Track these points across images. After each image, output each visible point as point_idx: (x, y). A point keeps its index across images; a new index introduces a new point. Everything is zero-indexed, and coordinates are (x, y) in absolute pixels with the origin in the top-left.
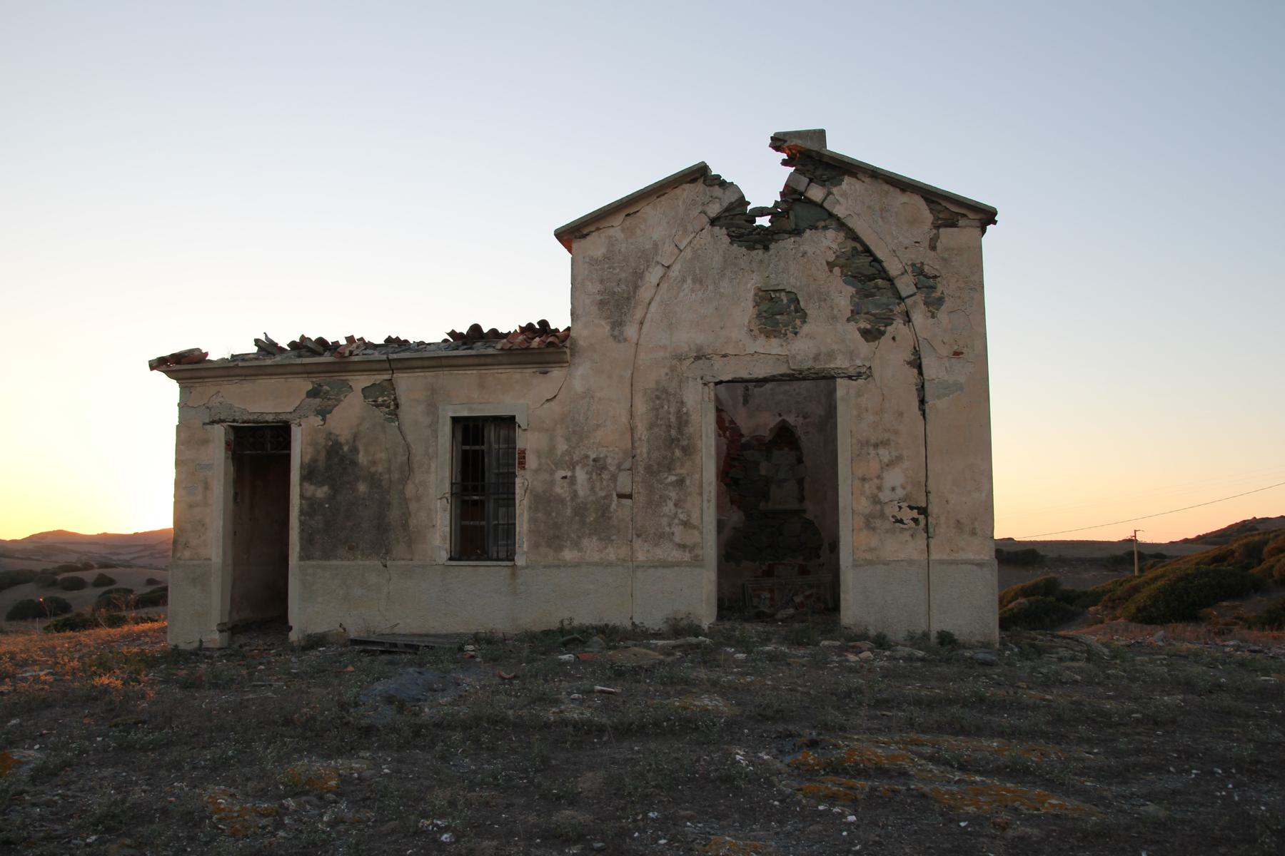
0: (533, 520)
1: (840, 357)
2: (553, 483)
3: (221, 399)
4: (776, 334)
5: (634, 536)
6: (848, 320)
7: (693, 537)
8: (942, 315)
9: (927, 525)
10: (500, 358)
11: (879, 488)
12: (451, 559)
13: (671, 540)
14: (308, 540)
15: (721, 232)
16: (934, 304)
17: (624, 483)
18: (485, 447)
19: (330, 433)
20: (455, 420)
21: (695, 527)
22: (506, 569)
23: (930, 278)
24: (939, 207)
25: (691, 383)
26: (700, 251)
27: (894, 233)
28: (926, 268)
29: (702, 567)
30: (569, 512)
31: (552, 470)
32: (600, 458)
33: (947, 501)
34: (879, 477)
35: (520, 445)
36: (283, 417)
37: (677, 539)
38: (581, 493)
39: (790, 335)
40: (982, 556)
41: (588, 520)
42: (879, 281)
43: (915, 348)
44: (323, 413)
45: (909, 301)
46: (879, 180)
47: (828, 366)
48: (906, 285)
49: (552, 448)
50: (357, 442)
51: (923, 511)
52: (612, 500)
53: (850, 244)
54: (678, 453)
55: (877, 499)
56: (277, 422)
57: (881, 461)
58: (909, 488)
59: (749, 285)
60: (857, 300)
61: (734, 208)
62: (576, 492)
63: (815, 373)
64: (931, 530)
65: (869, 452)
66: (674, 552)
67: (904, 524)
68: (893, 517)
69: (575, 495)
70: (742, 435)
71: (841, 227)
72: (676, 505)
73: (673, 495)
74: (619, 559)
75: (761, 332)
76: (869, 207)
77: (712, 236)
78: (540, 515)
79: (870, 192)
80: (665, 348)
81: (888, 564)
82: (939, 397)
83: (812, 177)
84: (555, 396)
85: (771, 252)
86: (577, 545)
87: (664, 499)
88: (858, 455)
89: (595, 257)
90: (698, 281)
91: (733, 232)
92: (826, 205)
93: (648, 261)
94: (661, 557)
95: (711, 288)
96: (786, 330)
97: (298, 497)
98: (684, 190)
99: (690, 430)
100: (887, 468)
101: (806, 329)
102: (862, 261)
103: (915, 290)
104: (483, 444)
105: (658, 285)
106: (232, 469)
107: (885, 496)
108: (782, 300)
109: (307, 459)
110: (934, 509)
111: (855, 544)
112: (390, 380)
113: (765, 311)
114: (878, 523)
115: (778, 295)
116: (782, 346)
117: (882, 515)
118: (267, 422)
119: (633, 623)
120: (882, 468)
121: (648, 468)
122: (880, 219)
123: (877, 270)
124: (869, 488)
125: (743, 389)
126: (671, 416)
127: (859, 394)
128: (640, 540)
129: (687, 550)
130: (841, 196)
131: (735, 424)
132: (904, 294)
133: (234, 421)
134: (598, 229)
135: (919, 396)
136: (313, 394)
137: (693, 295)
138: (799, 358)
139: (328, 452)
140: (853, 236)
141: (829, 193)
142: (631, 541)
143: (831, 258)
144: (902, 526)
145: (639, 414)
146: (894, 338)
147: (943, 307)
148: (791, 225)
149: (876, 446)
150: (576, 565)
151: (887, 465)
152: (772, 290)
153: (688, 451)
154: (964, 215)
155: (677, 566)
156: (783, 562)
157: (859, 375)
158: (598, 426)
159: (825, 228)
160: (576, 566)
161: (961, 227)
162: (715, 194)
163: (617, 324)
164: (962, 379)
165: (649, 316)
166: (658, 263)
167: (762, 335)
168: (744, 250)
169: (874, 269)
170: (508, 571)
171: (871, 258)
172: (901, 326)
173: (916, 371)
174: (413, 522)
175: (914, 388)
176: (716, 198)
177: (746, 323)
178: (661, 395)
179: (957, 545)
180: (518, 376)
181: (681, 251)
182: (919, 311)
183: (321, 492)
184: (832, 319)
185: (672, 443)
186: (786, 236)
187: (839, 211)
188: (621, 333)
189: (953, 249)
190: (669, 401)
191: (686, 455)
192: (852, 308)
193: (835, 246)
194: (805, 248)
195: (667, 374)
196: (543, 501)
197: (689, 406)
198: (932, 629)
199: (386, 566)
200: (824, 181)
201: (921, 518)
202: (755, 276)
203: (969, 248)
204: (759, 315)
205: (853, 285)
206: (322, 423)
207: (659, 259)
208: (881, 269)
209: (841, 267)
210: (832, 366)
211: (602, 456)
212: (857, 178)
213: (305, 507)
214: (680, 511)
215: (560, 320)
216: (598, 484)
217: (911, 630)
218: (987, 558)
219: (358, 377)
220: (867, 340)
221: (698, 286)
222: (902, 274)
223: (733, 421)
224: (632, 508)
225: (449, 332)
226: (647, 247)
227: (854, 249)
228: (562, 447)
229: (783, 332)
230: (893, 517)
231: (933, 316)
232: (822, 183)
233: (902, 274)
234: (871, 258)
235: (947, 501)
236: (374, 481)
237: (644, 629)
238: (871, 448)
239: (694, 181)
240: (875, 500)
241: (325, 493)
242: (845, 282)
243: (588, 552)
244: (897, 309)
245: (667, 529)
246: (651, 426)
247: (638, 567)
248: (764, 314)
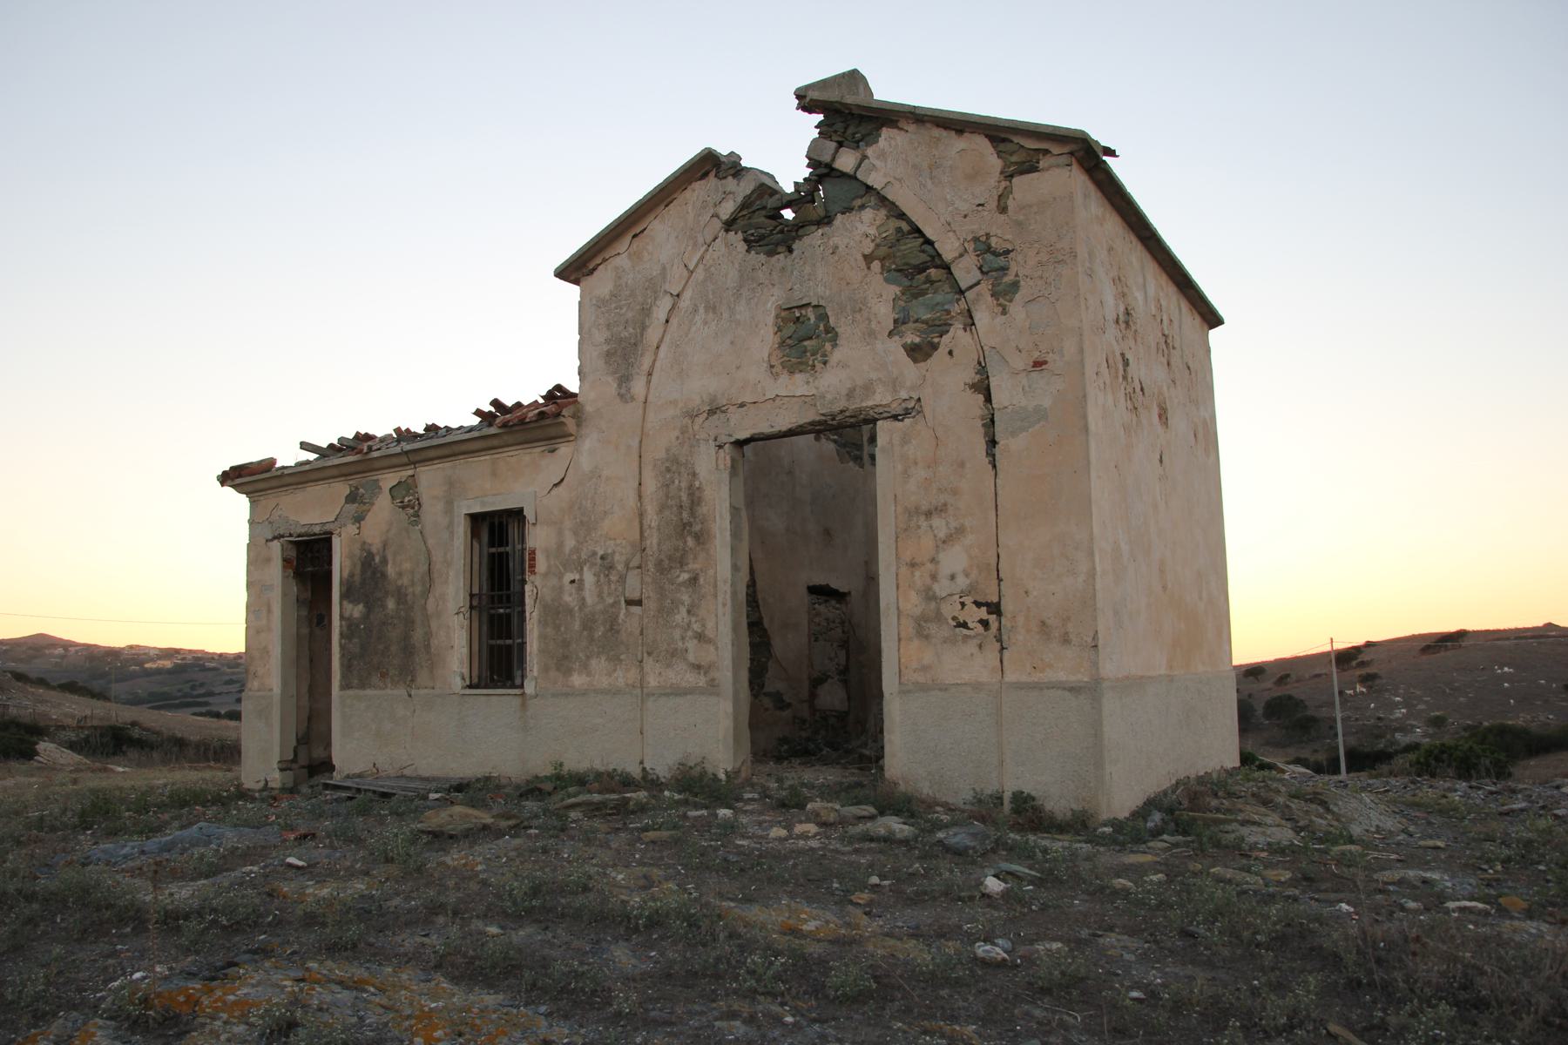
0: (543, 637)
1: (880, 389)
2: (561, 589)
3: (280, 513)
4: (802, 367)
5: (645, 655)
6: (891, 334)
7: (707, 655)
8: (1016, 308)
9: (999, 629)
10: (505, 437)
11: (934, 577)
12: (470, 686)
13: (685, 659)
14: (347, 668)
15: (736, 238)
16: (1004, 293)
17: (633, 587)
18: (508, 549)
19: (364, 543)
20: (476, 519)
21: (710, 641)
23: (1000, 255)
24: (1009, 147)
25: (703, 448)
26: (713, 269)
27: (948, 197)
28: (993, 242)
29: (718, 695)
30: (577, 626)
31: (560, 572)
32: (608, 554)
33: (1026, 592)
34: (933, 560)
37: (691, 657)
38: (589, 601)
39: (819, 366)
40: (1080, 677)
41: (596, 636)
42: (932, 271)
43: (979, 363)
44: (359, 519)
45: (970, 295)
46: (928, 125)
47: (864, 404)
48: (966, 272)
49: (560, 545)
51: (995, 609)
52: (620, 609)
53: (894, 223)
54: (690, 542)
55: (931, 593)
56: (324, 534)
57: (935, 536)
58: (974, 573)
59: (769, 305)
60: (902, 303)
61: (753, 202)
62: (583, 599)
63: (851, 417)
64: (1005, 637)
65: (920, 523)
66: (688, 676)
67: (968, 628)
68: (954, 618)
71: (882, 202)
72: (689, 612)
73: (686, 598)
74: (627, 685)
75: (784, 368)
76: (914, 166)
77: (726, 245)
78: (549, 630)
79: (916, 144)
80: (674, 403)
81: (946, 689)
82: (1013, 434)
83: (840, 139)
84: (562, 480)
85: (795, 253)
86: (585, 667)
87: (676, 603)
88: (906, 530)
89: (602, 296)
90: (712, 308)
91: (752, 235)
92: (859, 175)
93: (655, 292)
94: (674, 681)
96: (813, 361)
98: (694, 190)
99: (703, 510)
100: (945, 547)
101: (836, 356)
102: (909, 245)
103: (978, 275)
104: (507, 545)
105: (667, 321)
106: (295, 589)
107: (941, 588)
108: (809, 319)
109: (346, 575)
110: (1007, 606)
111: (903, 660)
112: (413, 476)
113: (790, 338)
114: (933, 628)
115: (803, 312)
116: (808, 383)
117: (939, 617)
118: (315, 534)
119: (644, 769)
120: (937, 546)
121: (659, 563)
122: (929, 182)
123: (931, 256)
124: (920, 577)
126: (682, 494)
127: (905, 440)
128: (651, 659)
129: (702, 672)
130: (878, 158)
132: (963, 286)
133: (291, 535)
134: (605, 260)
135: (986, 434)
136: (352, 498)
137: (706, 328)
138: (829, 397)
139: (363, 565)
141: (864, 157)
142: (641, 662)
143: (867, 251)
144: (965, 631)
145: (649, 493)
146: (950, 353)
147: (1018, 296)
148: (817, 209)
149: (929, 514)
150: (584, 693)
151: (944, 542)
152: (797, 307)
153: (702, 538)
155: (690, 694)
157: (907, 412)
159: (862, 207)
160: (584, 694)
161: (1043, 170)
162: (728, 189)
163: (624, 380)
164: (1047, 403)
165: (658, 364)
167: (785, 371)
168: (762, 257)
169: (925, 255)
170: (517, 702)
171: (921, 240)
172: (961, 333)
173: (981, 398)
174: (434, 642)
175: (979, 423)
176: (730, 193)
177: (766, 359)
178: (673, 466)
179: (1042, 660)
180: (527, 458)
181: (692, 272)
182: (984, 306)
184: (870, 335)
185: (685, 528)
186: (813, 228)
187: (875, 180)
188: (629, 390)
189: (1030, 206)
190: (679, 473)
191: (699, 544)
192: (897, 316)
193: (872, 231)
194: (835, 240)
195: (678, 438)
197: (701, 478)
198: (1005, 788)
199: (410, 696)
200: (858, 142)
201: (992, 618)
202: (777, 291)
203: (1055, 199)
204: (782, 344)
205: (899, 285)
207: (667, 287)
208: (934, 254)
209: (882, 260)
210: (870, 403)
211: (610, 551)
212: (901, 129)
213: (345, 629)
214: (693, 619)
215: (573, 385)
216: (606, 591)
217: (978, 789)
218: (1086, 679)
219: (386, 476)
220: (915, 361)
221: (711, 315)
222: (961, 255)
224: (641, 618)
225: (474, 411)
226: (655, 274)
227: (899, 230)
229: (811, 363)
230: (954, 618)
231: (1004, 312)
232: (856, 145)
233: (961, 255)
234: (921, 240)
235: (1026, 592)
237: (655, 777)
238: (922, 518)
239: (705, 175)
240: (929, 595)
242: (887, 280)
243: (597, 676)
244: (956, 309)
245: (680, 644)
246: (662, 508)
247: (649, 695)
248: (789, 341)
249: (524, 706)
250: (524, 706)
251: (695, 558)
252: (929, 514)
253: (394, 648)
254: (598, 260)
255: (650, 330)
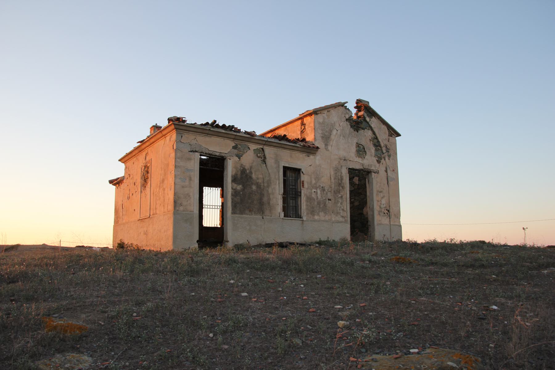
0: (307, 205)
2: (311, 193)
3: (196, 142)
7: (345, 214)
17: (330, 196)
19: (242, 165)
21: (345, 211)
22: (301, 221)
30: (316, 203)
35: (302, 179)
36: (223, 155)
38: (319, 197)
44: (239, 157)
49: (311, 182)
50: (252, 170)
51: (389, 211)
54: (341, 188)
56: (219, 156)
62: (318, 197)
69: (317, 198)
72: (341, 204)
73: (340, 200)
78: (308, 203)
86: (318, 214)
87: (338, 202)
90: (344, 136)
95: (347, 140)
97: (231, 188)
99: (343, 181)
107: (382, 206)
110: (391, 211)
114: (381, 213)
117: (381, 211)
121: (334, 191)
132: (384, 152)
134: (321, 113)
136: (235, 147)
139: (241, 172)
140: (374, 133)
149: (380, 192)
150: (319, 221)
153: (343, 187)
154: (393, 134)
158: (323, 176)
166: (335, 128)
170: (300, 222)
174: (271, 202)
180: (301, 156)
183: (239, 187)
187: (372, 126)
188: (327, 148)
194: (365, 134)
196: (309, 199)
199: (263, 218)
206: (239, 160)
207: (335, 127)
228: (314, 182)
236: (258, 185)
241: (241, 188)
246: (335, 179)
249: (303, 223)
250: (303, 223)
251: (342, 192)
252: (380, 192)
253: (255, 202)
254: (319, 112)
255: (332, 136)
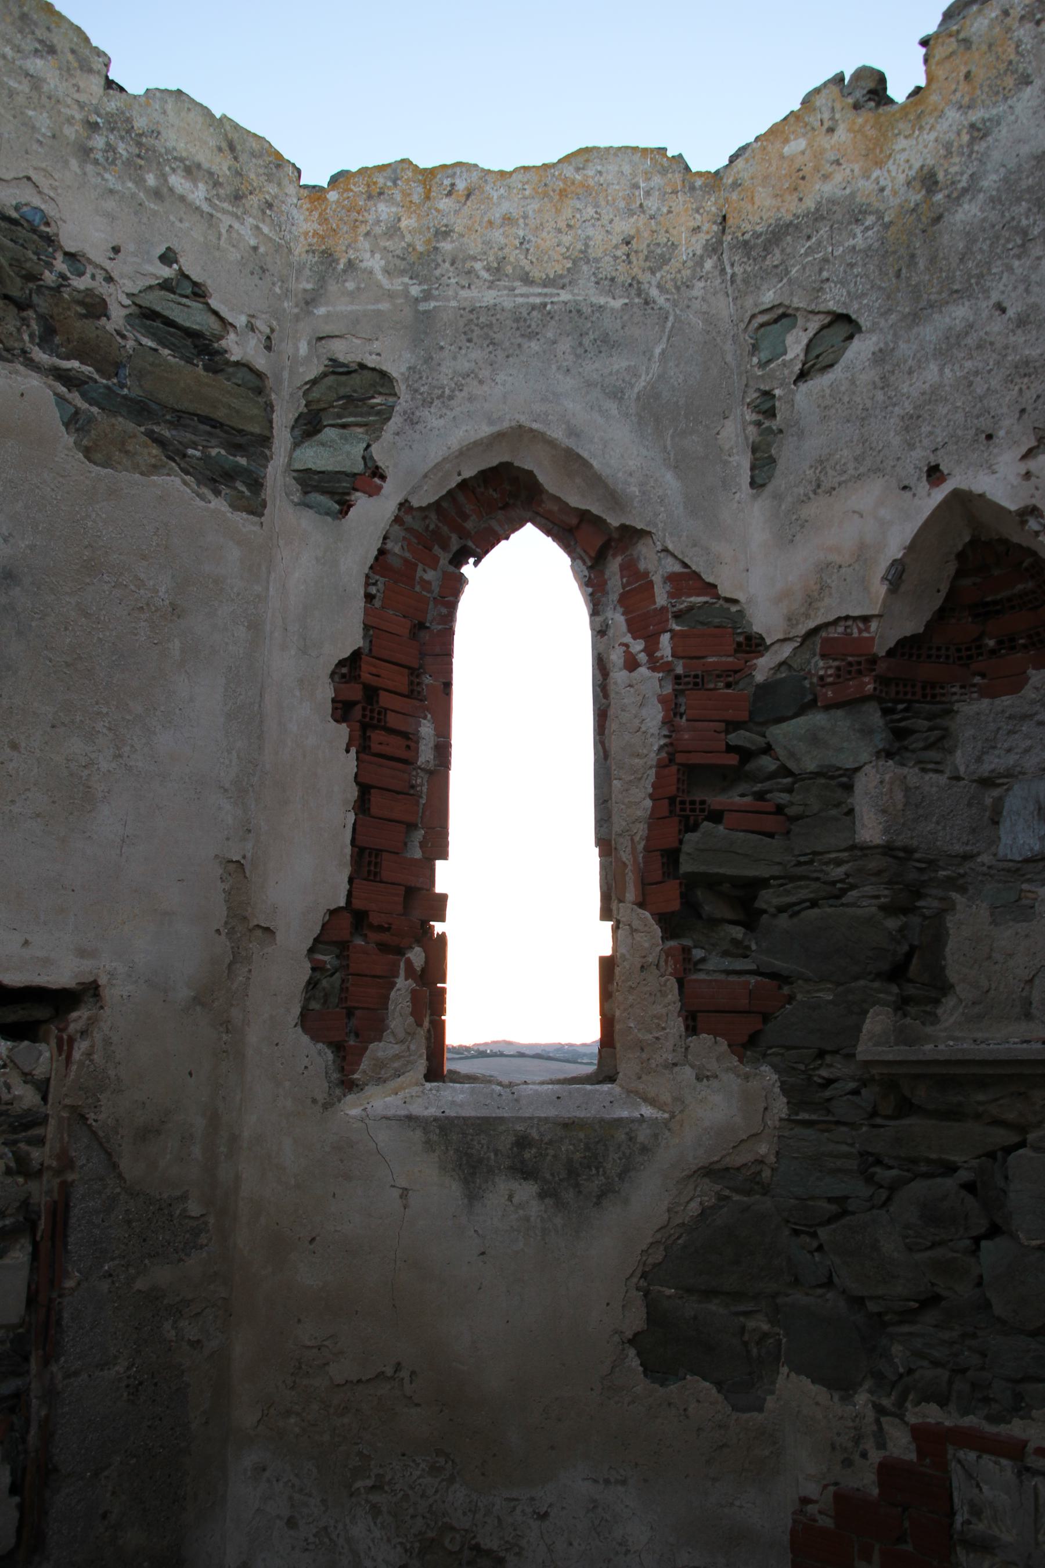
70: (754, 645)
125: (750, 416)
131: (711, 588)
156: (1016, 1429)
223: (697, 575)
